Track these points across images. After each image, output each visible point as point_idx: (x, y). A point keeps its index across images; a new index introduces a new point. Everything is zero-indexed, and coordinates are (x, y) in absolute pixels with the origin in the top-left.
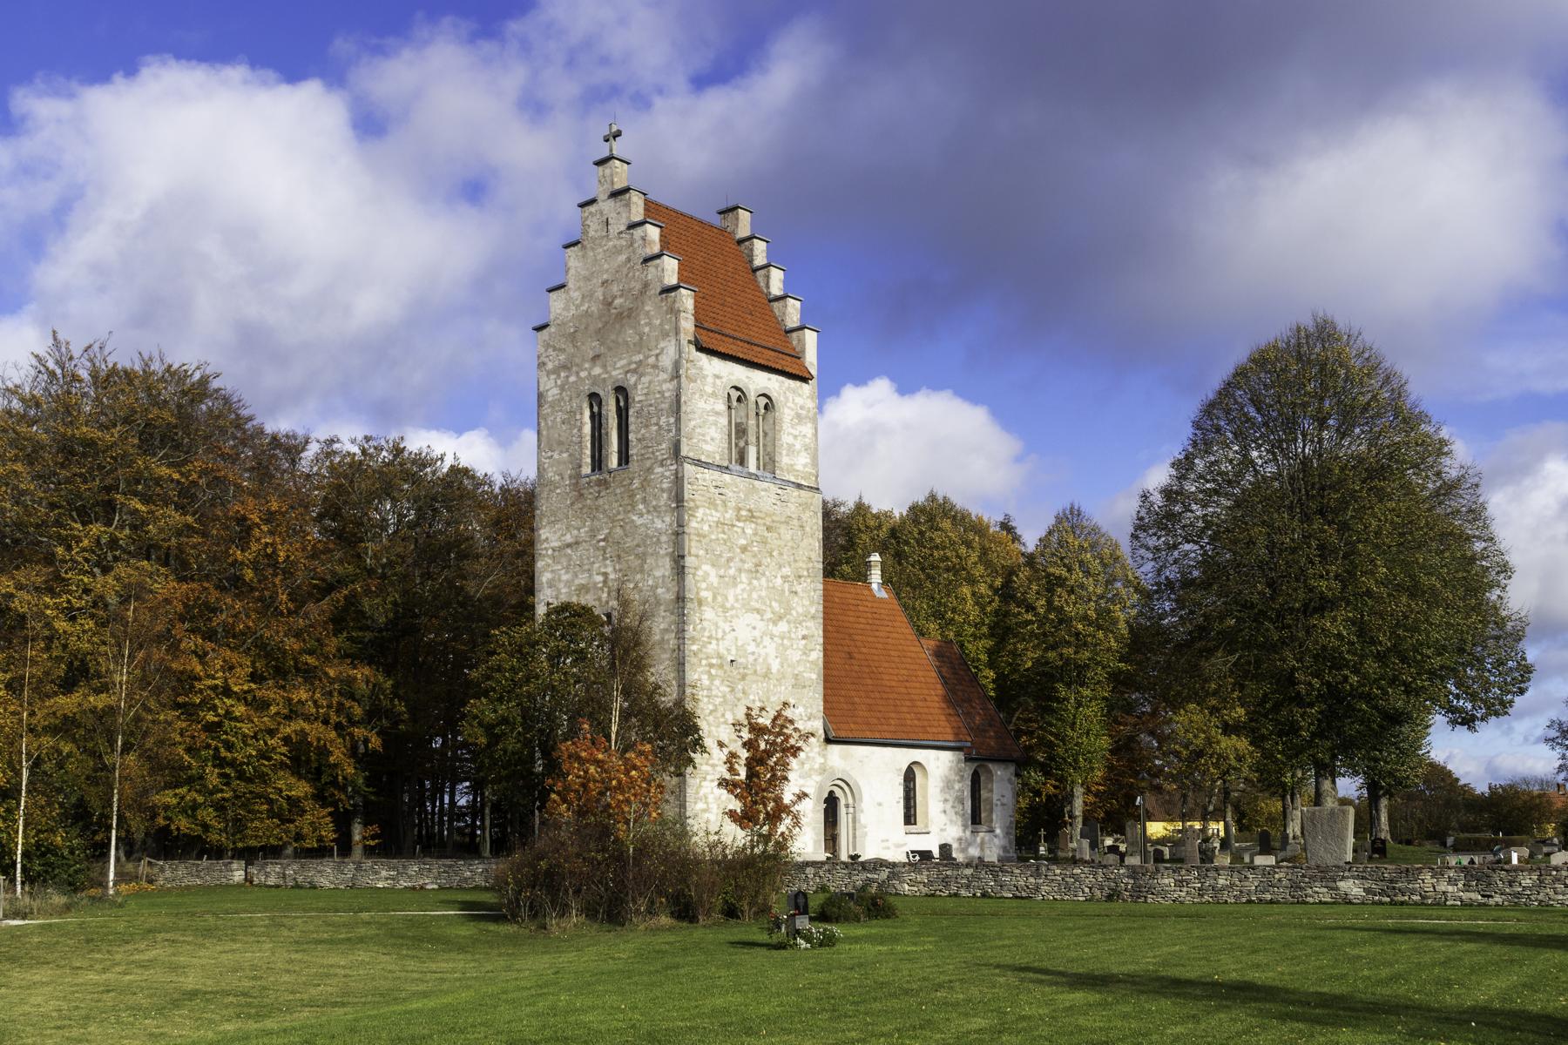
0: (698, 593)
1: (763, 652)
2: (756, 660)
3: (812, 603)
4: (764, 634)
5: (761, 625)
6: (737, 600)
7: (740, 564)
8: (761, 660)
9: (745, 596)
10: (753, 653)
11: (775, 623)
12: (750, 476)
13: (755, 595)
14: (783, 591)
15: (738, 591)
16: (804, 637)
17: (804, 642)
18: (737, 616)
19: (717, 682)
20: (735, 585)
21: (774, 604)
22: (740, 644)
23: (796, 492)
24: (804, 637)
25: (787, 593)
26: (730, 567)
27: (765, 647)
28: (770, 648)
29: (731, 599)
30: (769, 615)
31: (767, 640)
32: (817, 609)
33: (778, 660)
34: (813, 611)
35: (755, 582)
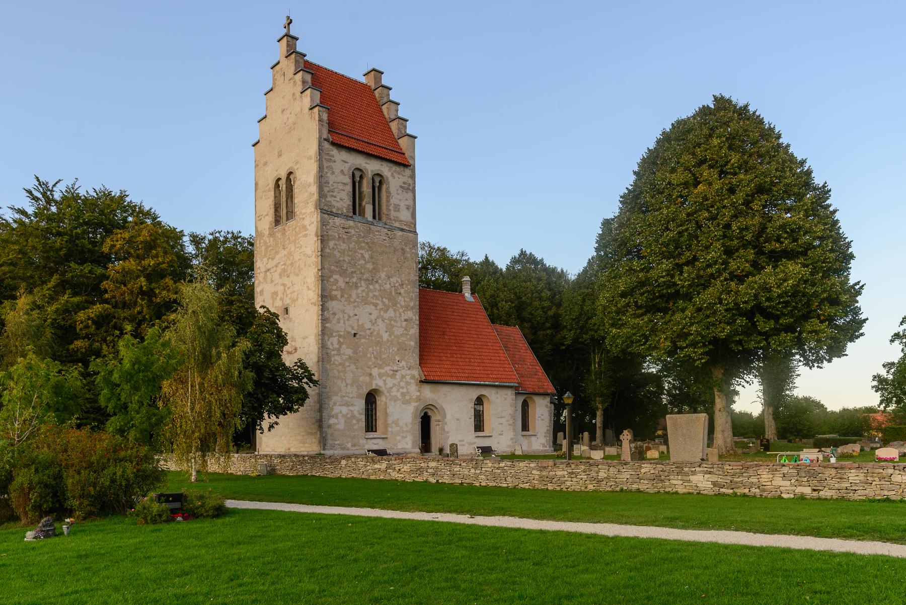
0: (330, 292)
1: (376, 328)
2: (371, 333)
3: (411, 300)
4: (378, 317)
5: (375, 313)
6: (358, 297)
7: (360, 276)
8: (375, 333)
9: (364, 294)
10: (370, 329)
11: (386, 311)
12: (368, 222)
13: (371, 295)
14: (391, 292)
15: (359, 291)
16: (406, 320)
17: (405, 323)
18: (358, 307)
19: (344, 346)
20: (357, 288)
21: (384, 299)
22: (360, 323)
23: (400, 233)
24: (406, 320)
25: (393, 294)
26: (353, 277)
27: (378, 325)
28: (381, 326)
29: (354, 296)
30: (380, 306)
31: (380, 322)
32: (414, 303)
33: (388, 333)
34: (412, 304)
35: (371, 287)
